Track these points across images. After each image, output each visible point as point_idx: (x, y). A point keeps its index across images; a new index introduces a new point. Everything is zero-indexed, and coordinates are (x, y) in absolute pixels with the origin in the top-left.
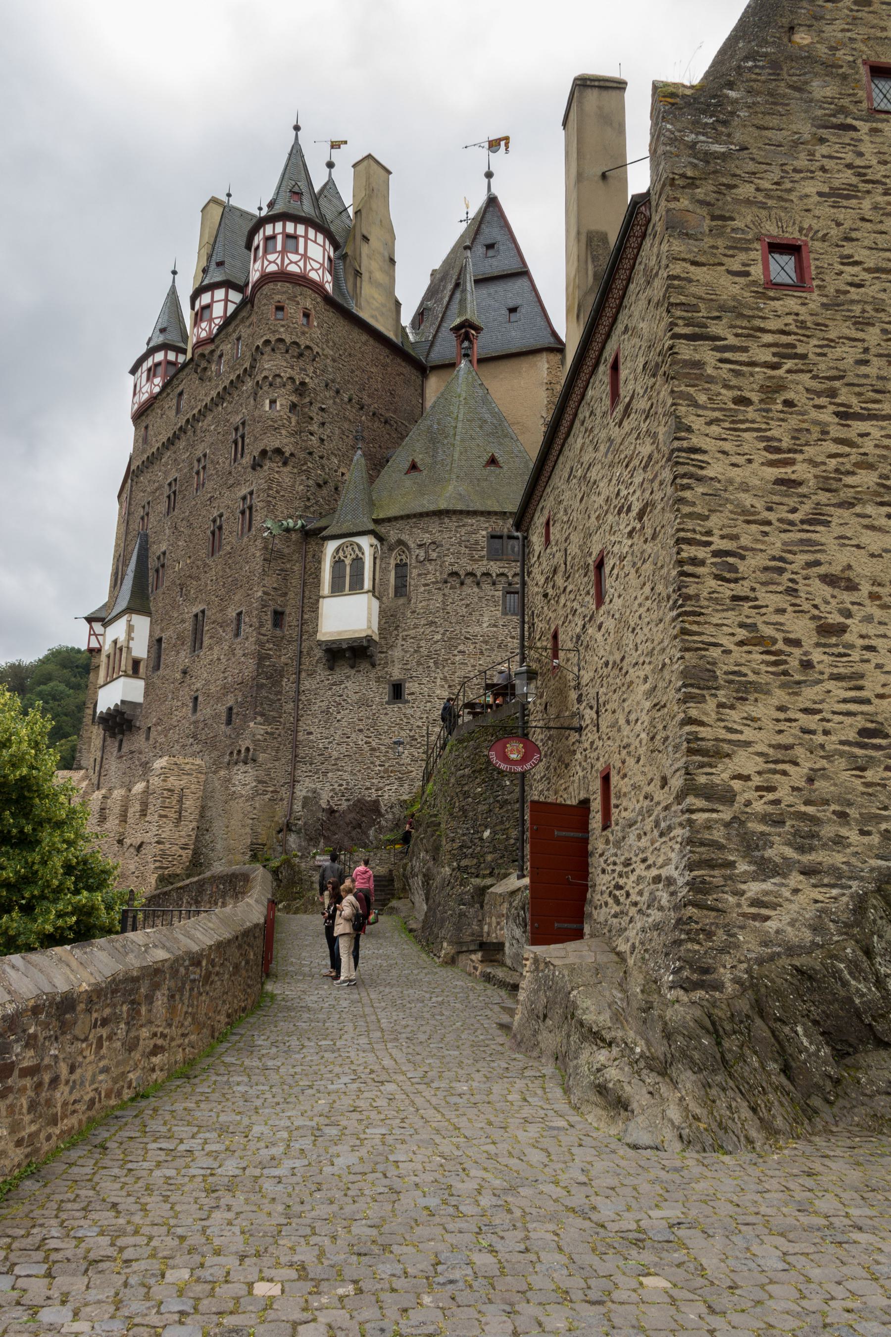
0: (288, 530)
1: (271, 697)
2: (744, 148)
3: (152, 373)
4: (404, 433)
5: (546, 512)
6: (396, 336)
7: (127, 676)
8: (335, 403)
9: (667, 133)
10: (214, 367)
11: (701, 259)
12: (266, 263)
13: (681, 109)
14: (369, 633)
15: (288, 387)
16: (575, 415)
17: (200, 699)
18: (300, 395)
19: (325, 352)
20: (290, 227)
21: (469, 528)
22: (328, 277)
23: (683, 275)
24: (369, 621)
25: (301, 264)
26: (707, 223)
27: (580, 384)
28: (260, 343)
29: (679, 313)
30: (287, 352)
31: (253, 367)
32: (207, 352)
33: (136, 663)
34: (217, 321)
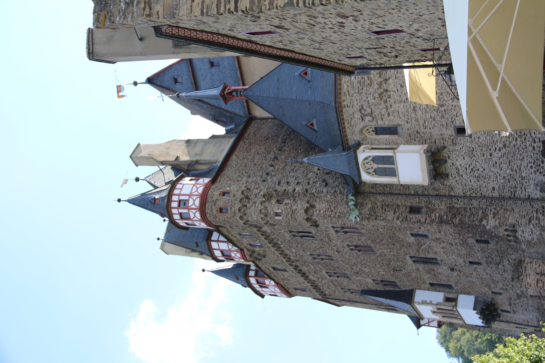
0: (356, 205)
1: (468, 214)
3: (262, 285)
4: (290, 130)
5: (341, 59)
6: (231, 137)
7: (456, 306)
8: (275, 176)
9: (122, 20)
10: (257, 249)
12: (195, 219)
13: (108, 13)
14: (422, 151)
15: (267, 205)
16: (281, 49)
17: (471, 260)
18: (271, 197)
19: (245, 182)
20: (174, 204)
21: (350, 88)
22: (201, 181)
23: (200, 7)
24: (413, 152)
25: (194, 197)
27: (262, 49)
28: (242, 222)
29: (222, 9)
30: (246, 206)
31: (256, 226)
32: (249, 253)
33: (447, 300)
34: (230, 247)
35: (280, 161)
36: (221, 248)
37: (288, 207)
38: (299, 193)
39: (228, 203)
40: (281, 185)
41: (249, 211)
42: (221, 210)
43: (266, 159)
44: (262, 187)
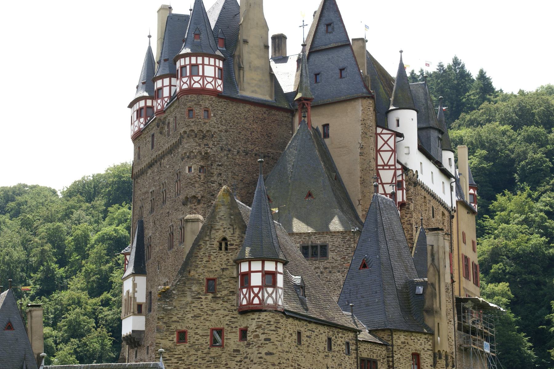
2: (175, 307)
6: (271, 97)
7: (134, 314)
8: (228, 158)
11: (163, 338)
12: (182, 83)
15: (199, 157)
18: (206, 159)
22: (220, 82)
25: (201, 82)
26: (166, 328)
28: (182, 131)
32: (162, 118)
33: (140, 306)
35: (244, 159)
36: (164, 88)
37: (197, 179)
38: (210, 188)
39: (198, 118)
40: (218, 167)
41: (192, 140)
42: (190, 110)
43: (245, 143)
44: (215, 149)
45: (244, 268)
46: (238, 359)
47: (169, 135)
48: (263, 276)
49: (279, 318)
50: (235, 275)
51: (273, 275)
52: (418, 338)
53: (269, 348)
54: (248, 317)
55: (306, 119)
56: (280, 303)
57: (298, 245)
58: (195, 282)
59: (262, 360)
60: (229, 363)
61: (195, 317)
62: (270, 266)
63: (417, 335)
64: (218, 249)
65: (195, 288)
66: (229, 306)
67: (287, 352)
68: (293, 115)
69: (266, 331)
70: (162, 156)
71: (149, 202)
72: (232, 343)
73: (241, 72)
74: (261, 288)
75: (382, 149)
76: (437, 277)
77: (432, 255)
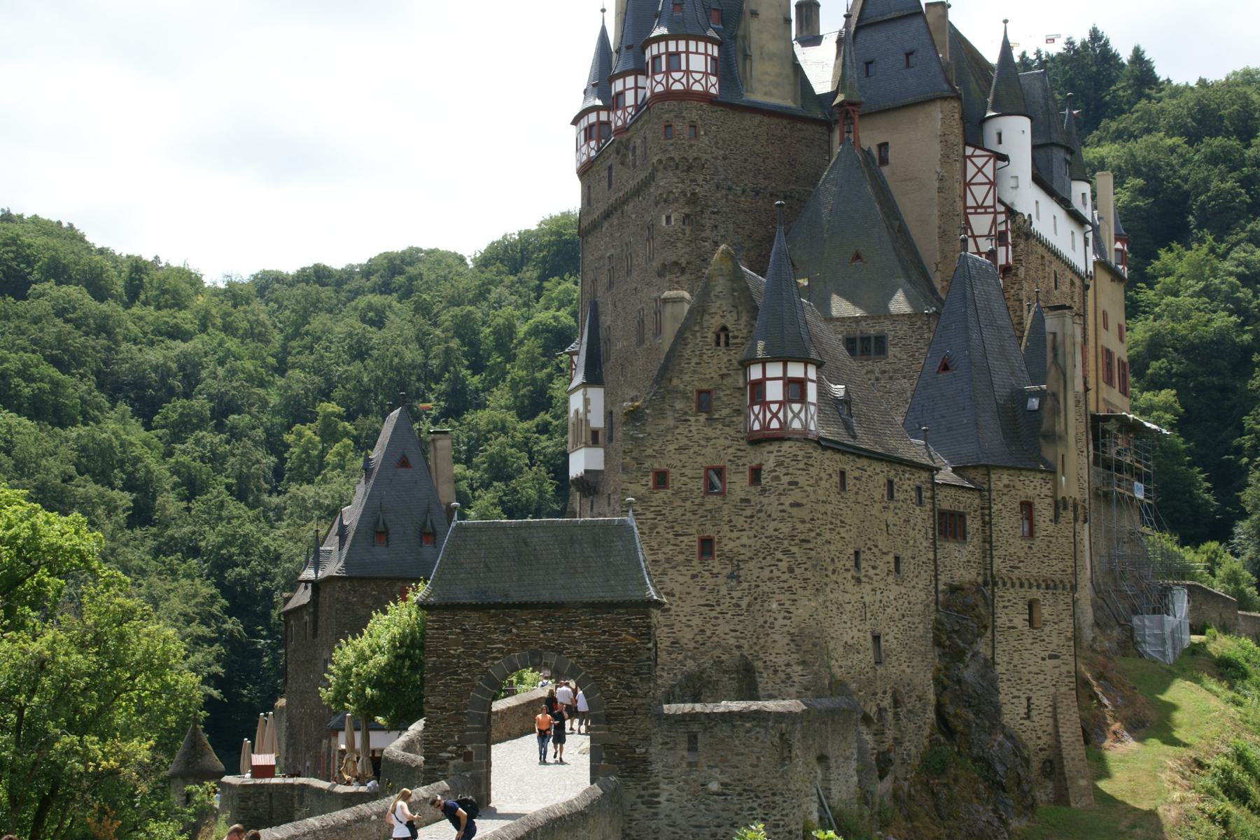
2: (649, 434)
3: (589, 133)
6: (795, 103)
8: (727, 201)
12: (654, 83)
20: (672, 46)
22: (713, 79)
25: (684, 80)
28: (655, 160)
30: (677, 168)
32: (624, 140)
40: (713, 216)
42: (668, 126)
43: (755, 176)
44: (706, 187)
45: (755, 373)
46: (748, 513)
47: (634, 166)
48: (784, 385)
49: (811, 451)
50: (741, 384)
51: (801, 383)
52: (1031, 478)
53: (796, 495)
54: (763, 449)
55: (851, 136)
56: (812, 427)
57: (840, 336)
58: (679, 395)
59: (786, 515)
60: (734, 518)
61: (681, 449)
62: (796, 371)
63: (1028, 474)
64: (713, 344)
65: (679, 405)
66: (732, 433)
67: (823, 502)
68: (831, 130)
69: (791, 470)
70: (625, 201)
71: (606, 272)
72: (738, 489)
73: (748, 62)
74: (782, 404)
75: (973, 182)
76: (1062, 382)
77: (1055, 349)
